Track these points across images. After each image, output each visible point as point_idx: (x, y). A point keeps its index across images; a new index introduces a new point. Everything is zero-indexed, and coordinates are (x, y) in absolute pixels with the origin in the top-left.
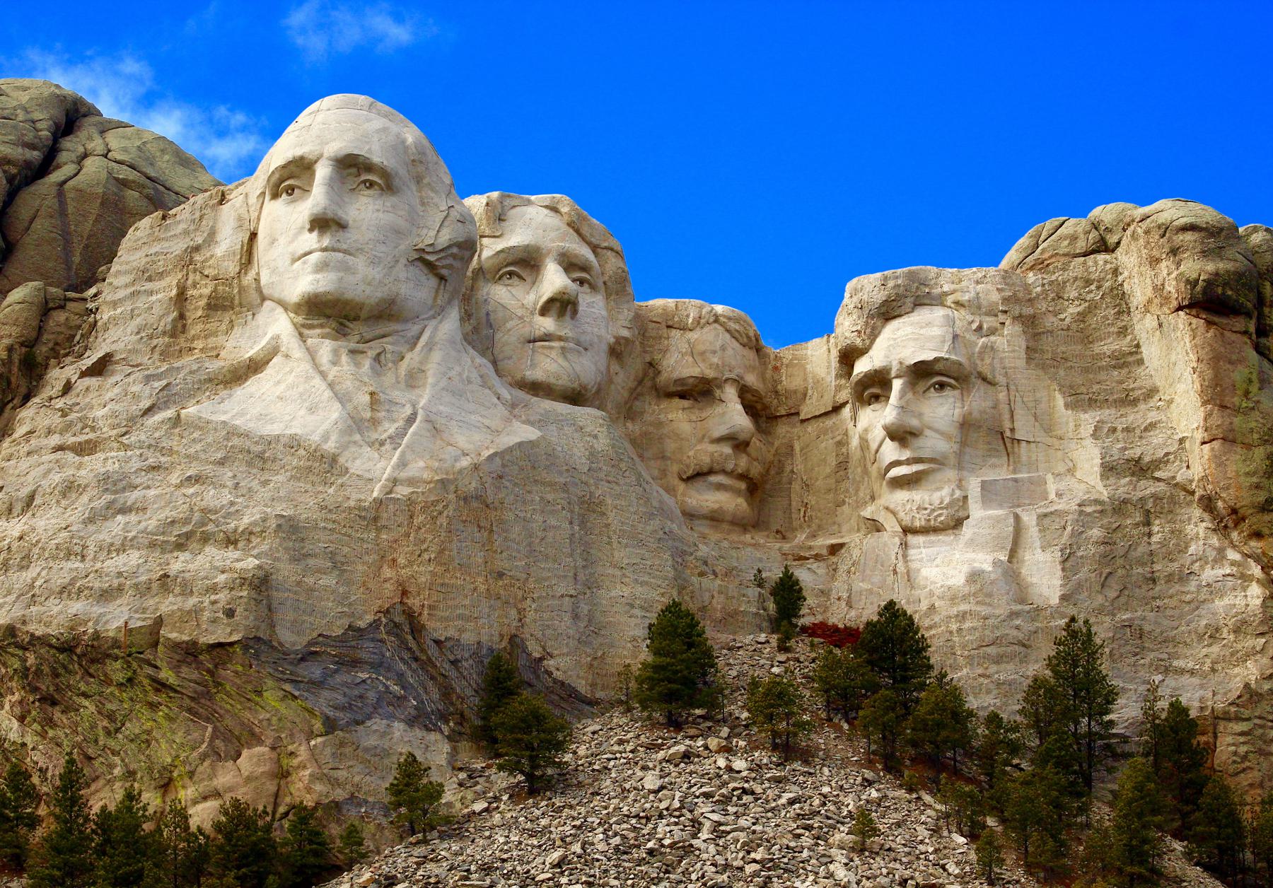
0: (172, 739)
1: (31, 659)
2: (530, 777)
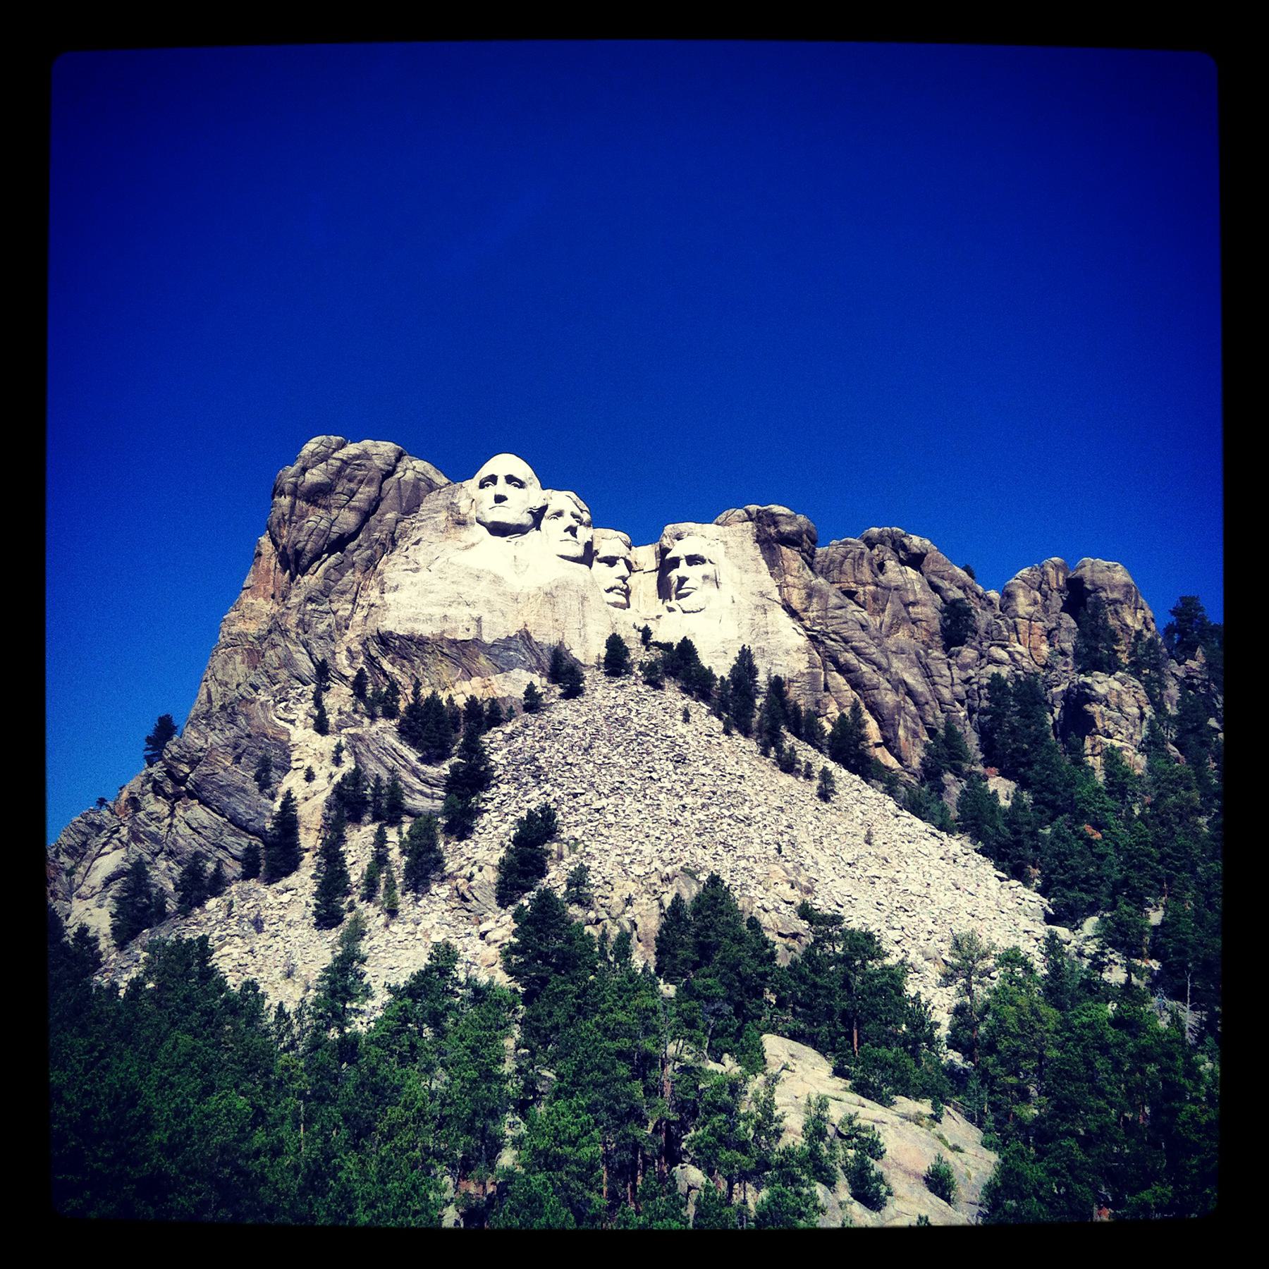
1: (397, 643)
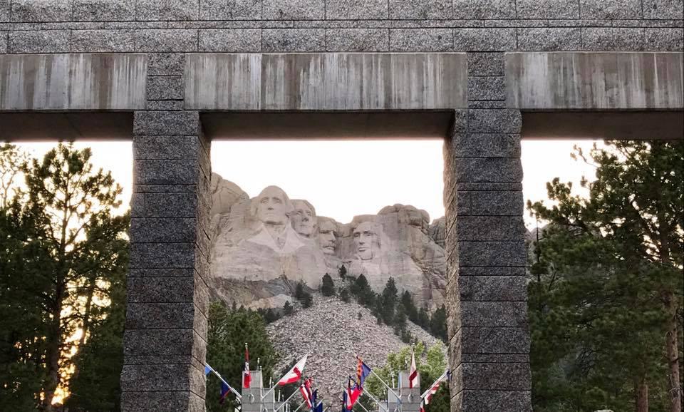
0: (247, 296)
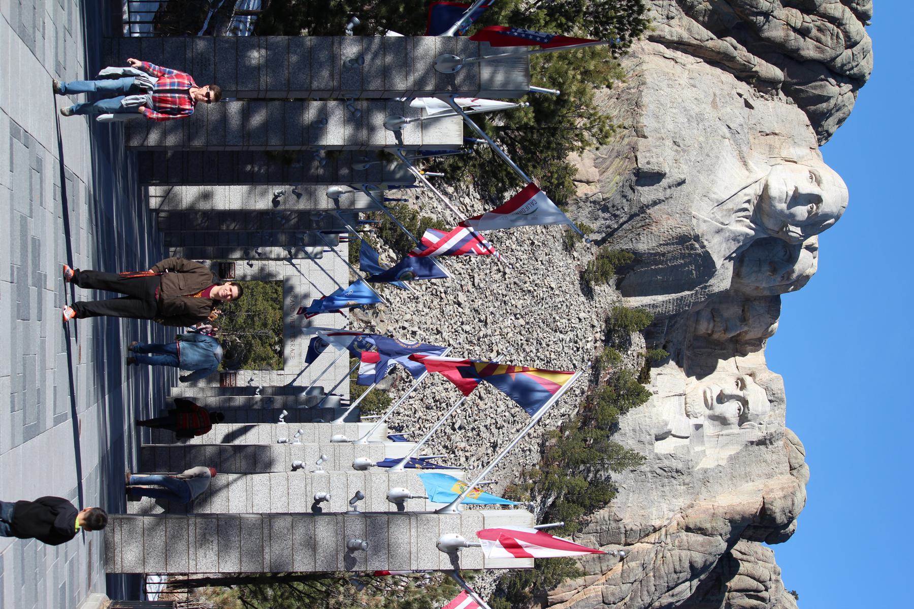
2: (585, 272)
